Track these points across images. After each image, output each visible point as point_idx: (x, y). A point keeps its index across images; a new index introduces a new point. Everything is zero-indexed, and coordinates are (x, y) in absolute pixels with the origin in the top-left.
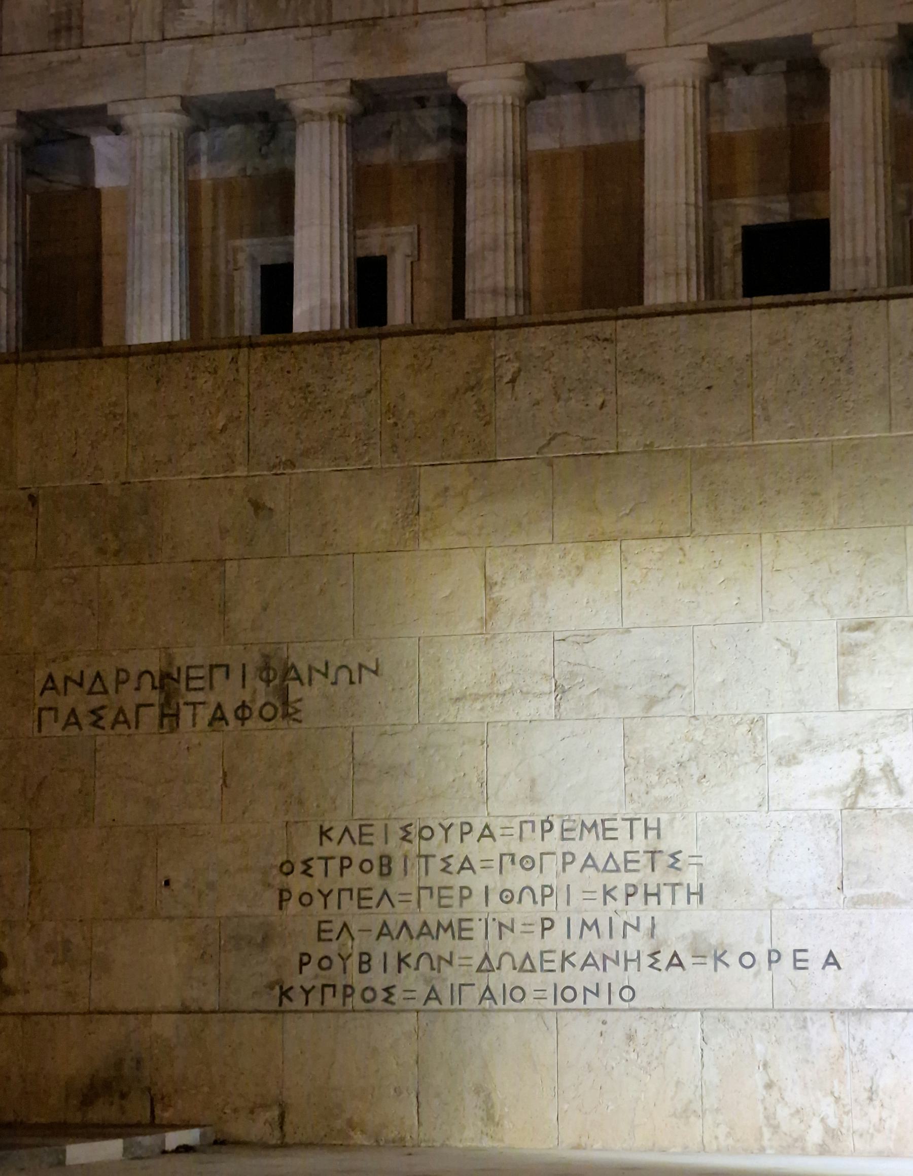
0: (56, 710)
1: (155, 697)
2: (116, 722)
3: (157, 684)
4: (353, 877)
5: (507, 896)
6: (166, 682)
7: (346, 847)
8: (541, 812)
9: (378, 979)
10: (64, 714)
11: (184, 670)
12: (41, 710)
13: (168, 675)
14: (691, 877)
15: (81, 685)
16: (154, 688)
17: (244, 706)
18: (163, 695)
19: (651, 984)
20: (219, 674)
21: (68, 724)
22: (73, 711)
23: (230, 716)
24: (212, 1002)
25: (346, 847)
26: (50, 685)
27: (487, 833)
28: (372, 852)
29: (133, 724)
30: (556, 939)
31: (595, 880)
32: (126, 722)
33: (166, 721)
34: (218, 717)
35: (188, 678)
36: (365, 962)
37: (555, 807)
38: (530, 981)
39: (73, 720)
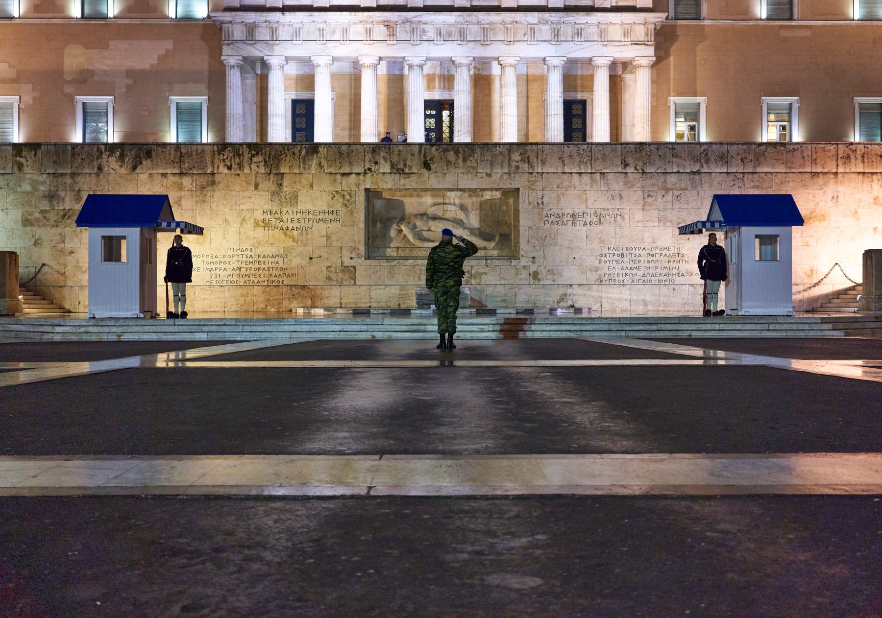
4: (616, 258)
5: (648, 262)
6: (573, 215)
7: (614, 252)
8: (655, 245)
9: (621, 278)
14: (686, 258)
19: (678, 280)
25: (614, 252)
27: (644, 249)
28: (620, 253)
30: (658, 270)
31: (666, 259)
34: (585, 224)
36: (618, 275)
37: (658, 244)
38: (653, 279)
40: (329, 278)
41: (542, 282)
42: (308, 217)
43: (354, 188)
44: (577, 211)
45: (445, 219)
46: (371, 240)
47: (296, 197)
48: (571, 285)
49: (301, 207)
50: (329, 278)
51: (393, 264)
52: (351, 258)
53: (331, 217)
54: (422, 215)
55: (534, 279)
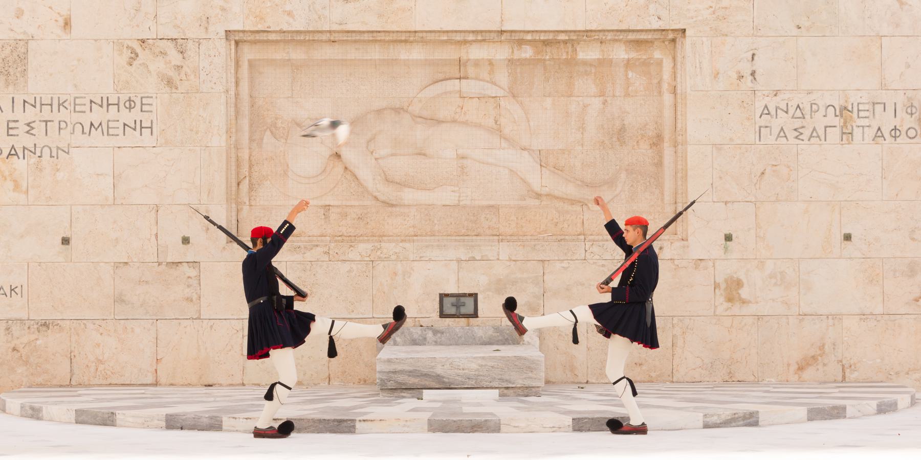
0: (770, 127)
1: (837, 121)
2: (811, 136)
3: (838, 113)
10: (776, 131)
11: (855, 105)
12: (760, 127)
13: (845, 108)
15: (787, 112)
16: (836, 116)
17: (895, 129)
18: (842, 120)
20: (879, 108)
21: (778, 136)
22: (782, 129)
23: (887, 135)
24: (879, 310)
26: (766, 111)
29: (823, 138)
32: (818, 136)
33: (844, 136)
35: (859, 110)
39: (782, 134)
40: (119, 299)
41: (752, 309)
42: (56, 116)
43: (193, 33)
44: (854, 98)
45: (466, 123)
46: (245, 186)
47: (23, 58)
48: (837, 317)
49: (38, 85)
50: (119, 299)
51: (309, 256)
52: (186, 241)
53: (127, 117)
54: (398, 110)
55: (730, 300)
